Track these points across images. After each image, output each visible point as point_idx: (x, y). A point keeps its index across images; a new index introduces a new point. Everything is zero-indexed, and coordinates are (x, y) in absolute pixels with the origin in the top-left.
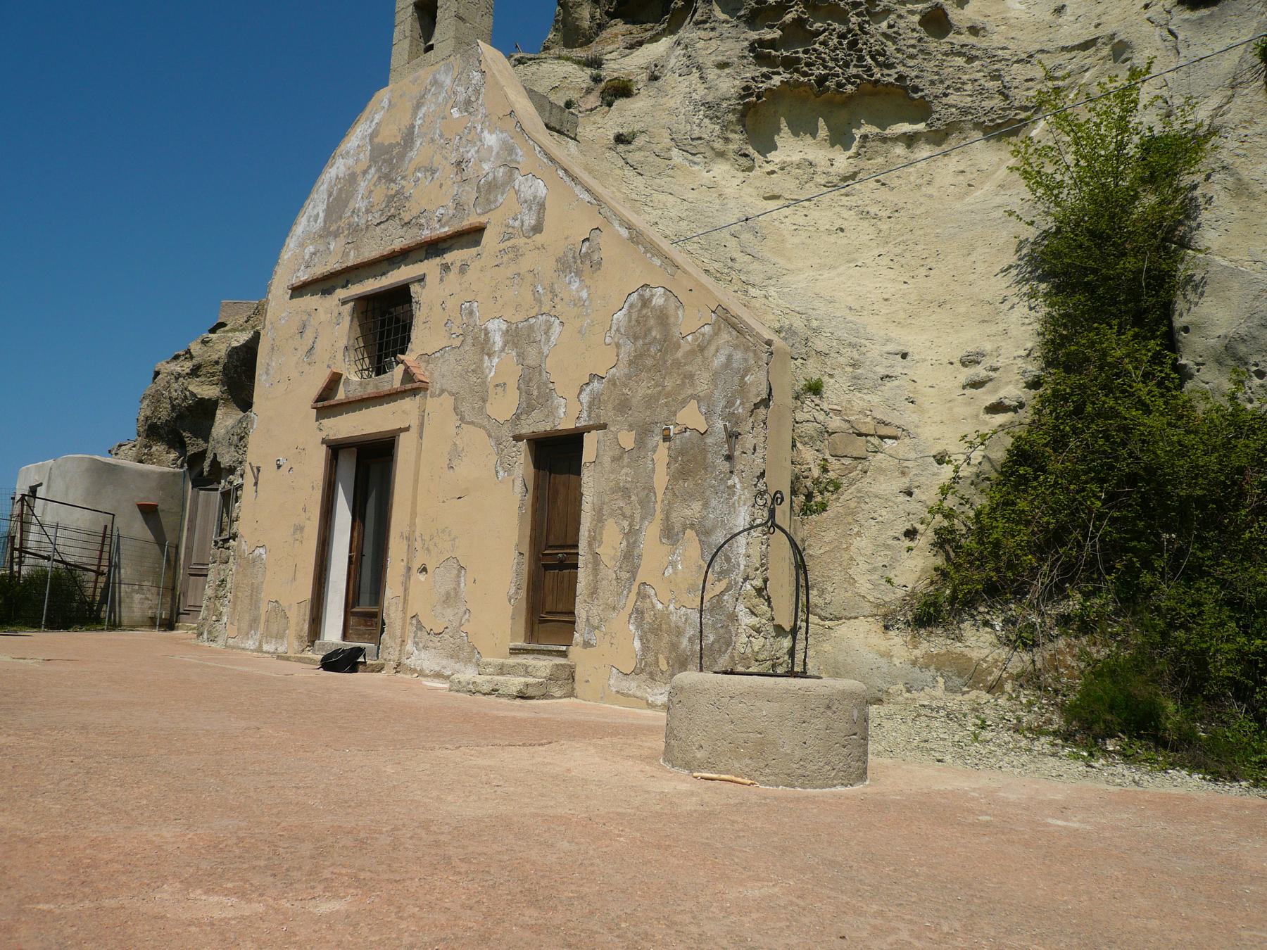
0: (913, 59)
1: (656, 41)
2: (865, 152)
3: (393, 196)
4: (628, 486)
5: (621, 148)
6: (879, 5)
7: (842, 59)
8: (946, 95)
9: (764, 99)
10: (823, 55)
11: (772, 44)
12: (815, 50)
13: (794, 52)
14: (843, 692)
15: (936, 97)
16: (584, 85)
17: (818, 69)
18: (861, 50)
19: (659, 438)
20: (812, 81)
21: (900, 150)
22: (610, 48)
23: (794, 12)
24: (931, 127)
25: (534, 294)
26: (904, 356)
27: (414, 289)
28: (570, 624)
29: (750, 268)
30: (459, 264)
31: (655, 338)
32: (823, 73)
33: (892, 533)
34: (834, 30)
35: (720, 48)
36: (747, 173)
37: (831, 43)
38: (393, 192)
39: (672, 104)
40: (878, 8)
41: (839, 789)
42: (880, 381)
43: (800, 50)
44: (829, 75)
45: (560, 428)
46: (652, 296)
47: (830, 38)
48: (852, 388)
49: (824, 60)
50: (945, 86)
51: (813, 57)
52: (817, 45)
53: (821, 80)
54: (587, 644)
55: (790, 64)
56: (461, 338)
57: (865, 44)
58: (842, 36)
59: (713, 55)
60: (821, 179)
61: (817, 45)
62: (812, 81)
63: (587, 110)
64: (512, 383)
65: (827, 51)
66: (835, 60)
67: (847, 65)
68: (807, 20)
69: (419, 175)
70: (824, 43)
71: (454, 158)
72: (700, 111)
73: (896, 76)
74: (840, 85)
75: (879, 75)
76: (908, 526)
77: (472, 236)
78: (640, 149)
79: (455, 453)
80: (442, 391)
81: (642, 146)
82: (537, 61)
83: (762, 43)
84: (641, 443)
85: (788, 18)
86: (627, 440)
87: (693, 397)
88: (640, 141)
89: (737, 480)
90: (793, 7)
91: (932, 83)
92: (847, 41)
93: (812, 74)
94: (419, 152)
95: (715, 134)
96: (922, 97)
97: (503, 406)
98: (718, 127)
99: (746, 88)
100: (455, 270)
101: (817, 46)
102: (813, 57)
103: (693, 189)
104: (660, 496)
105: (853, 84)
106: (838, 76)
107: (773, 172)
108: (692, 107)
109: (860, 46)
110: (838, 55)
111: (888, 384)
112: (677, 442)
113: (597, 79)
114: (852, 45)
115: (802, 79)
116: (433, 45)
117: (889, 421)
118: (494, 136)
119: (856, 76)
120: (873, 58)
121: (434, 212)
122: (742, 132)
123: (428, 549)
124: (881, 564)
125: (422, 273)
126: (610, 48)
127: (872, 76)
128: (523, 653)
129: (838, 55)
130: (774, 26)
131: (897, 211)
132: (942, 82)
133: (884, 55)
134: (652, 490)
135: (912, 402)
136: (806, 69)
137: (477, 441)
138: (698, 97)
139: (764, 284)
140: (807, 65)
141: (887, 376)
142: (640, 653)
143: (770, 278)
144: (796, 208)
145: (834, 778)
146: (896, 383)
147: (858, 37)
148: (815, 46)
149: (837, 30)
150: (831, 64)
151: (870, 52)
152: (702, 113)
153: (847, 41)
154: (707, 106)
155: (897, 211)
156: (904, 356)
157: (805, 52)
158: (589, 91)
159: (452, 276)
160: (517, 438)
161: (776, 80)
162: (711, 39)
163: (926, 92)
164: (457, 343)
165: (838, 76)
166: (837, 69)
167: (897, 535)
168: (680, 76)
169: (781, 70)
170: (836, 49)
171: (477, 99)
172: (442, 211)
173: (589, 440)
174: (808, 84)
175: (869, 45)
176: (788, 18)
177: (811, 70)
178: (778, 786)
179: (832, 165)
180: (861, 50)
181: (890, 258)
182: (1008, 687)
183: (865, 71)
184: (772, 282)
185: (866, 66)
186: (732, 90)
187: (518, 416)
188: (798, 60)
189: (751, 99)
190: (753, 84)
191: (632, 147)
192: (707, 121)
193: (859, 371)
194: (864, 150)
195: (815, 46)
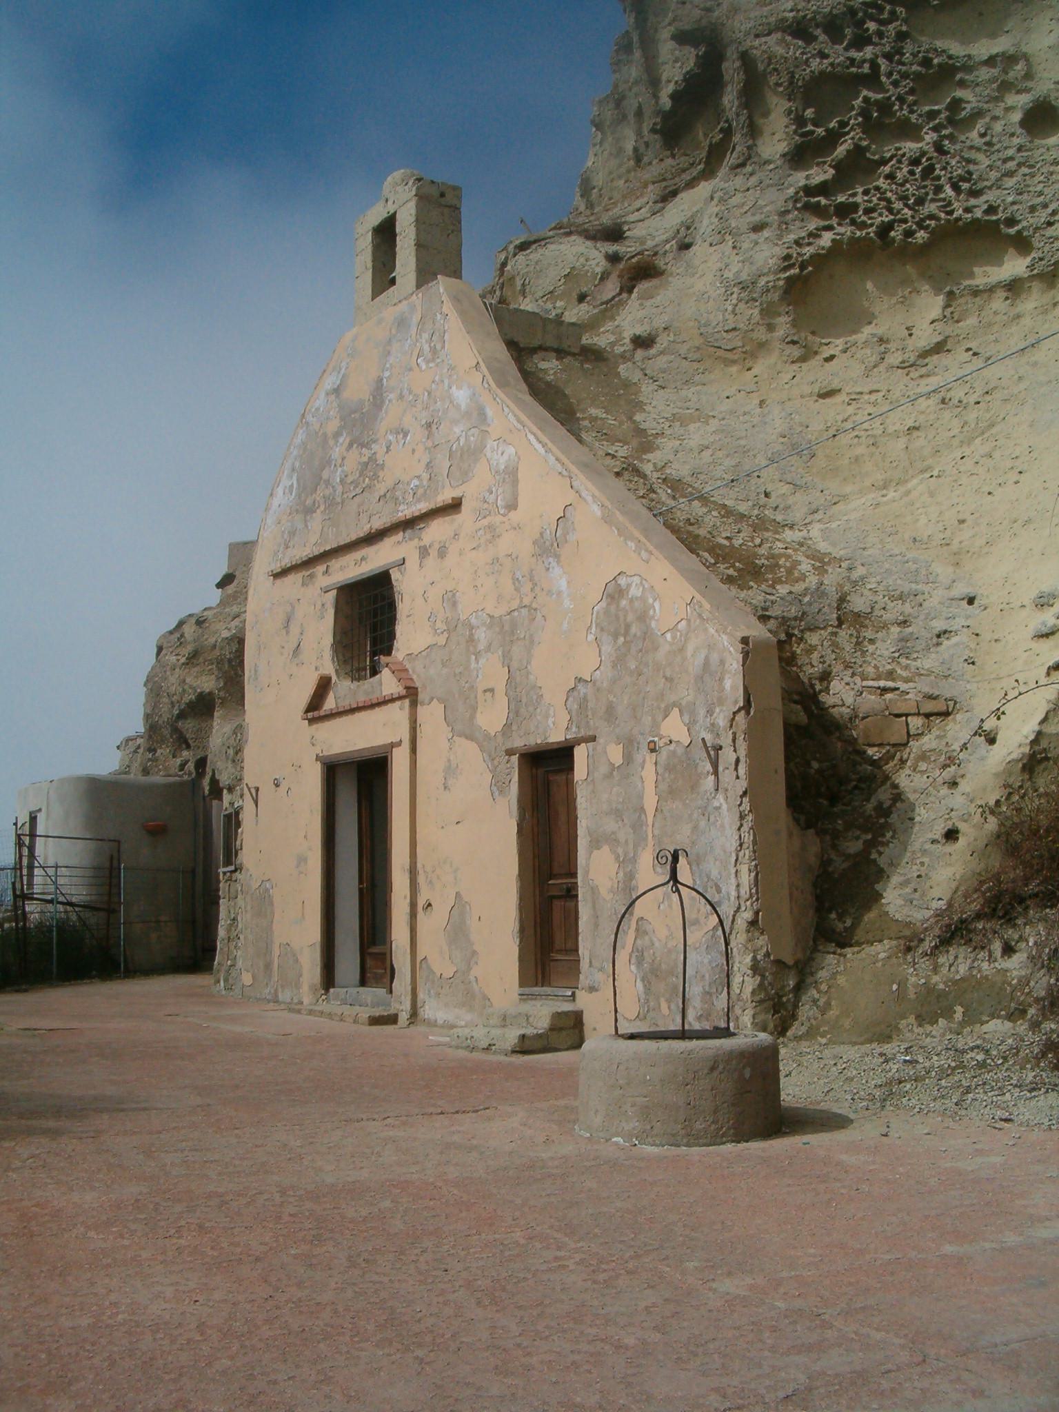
0: (1012, 176)
1: (693, 187)
2: (952, 313)
3: (366, 464)
4: (620, 807)
5: (640, 354)
6: (965, 108)
7: (914, 195)
8: (1050, 224)
9: (810, 268)
10: (889, 194)
11: (824, 189)
12: (877, 188)
13: (850, 195)
14: (731, 1052)
15: (1037, 229)
16: (599, 270)
17: (881, 215)
18: (939, 178)
19: (644, 750)
20: (872, 235)
21: (998, 303)
22: (638, 204)
23: (849, 141)
24: (1032, 270)
25: (514, 584)
26: (971, 601)
27: (395, 575)
28: (574, 967)
29: (791, 501)
30: (437, 546)
31: (635, 635)
32: (887, 220)
33: (931, 836)
34: (904, 155)
35: (761, 202)
36: (799, 365)
37: (899, 175)
38: (365, 459)
39: (699, 286)
40: (964, 113)
41: (729, 1146)
42: (935, 640)
43: (860, 190)
44: (894, 221)
45: (551, 740)
46: (629, 586)
47: (898, 168)
48: (897, 655)
49: (889, 201)
50: (1049, 210)
51: (874, 199)
52: (882, 180)
53: (885, 230)
54: (592, 989)
55: (845, 211)
56: (446, 635)
57: (944, 168)
58: (915, 162)
59: (749, 213)
60: (894, 359)
61: (882, 180)
62: (872, 235)
63: (602, 304)
64: (501, 687)
65: (894, 187)
66: (904, 198)
67: (920, 201)
68: (867, 148)
69: (391, 437)
70: (891, 177)
71: (424, 417)
72: (732, 294)
73: (985, 207)
74: (909, 233)
75: (961, 211)
76: (949, 825)
77: (455, 506)
78: (662, 353)
79: (450, 771)
80: (432, 699)
81: (665, 349)
82: (543, 243)
83: (809, 191)
84: (628, 758)
85: (841, 150)
86: (615, 754)
87: (674, 705)
88: (663, 341)
89: (722, 800)
90: (848, 133)
91: (1033, 209)
92: (920, 168)
93: (872, 225)
94: (392, 414)
95: (752, 322)
96: (1019, 232)
97: (492, 717)
98: (756, 311)
99: (787, 257)
100: (433, 553)
101: (881, 183)
102: (874, 199)
103: (728, 397)
104: (650, 820)
105: (926, 228)
106: (905, 221)
107: (832, 358)
108: (724, 290)
109: (937, 172)
110: (908, 190)
111: (946, 642)
112: (664, 753)
113: (614, 259)
114: (928, 171)
115: (858, 233)
116: (394, 277)
117: (937, 693)
118: (461, 392)
119: (931, 217)
120: (955, 187)
121: (408, 484)
122: (787, 313)
123: (431, 882)
124: (915, 875)
125: (401, 557)
126: (638, 204)
127: (951, 213)
128: (532, 999)
129: (908, 190)
130: (825, 163)
131: (987, 393)
132: (1045, 206)
133: (968, 181)
134: (642, 809)
135: (973, 663)
136: (864, 218)
137: (469, 754)
138: (731, 275)
139: (807, 521)
140: (868, 211)
141: (945, 632)
142: (643, 996)
143: (816, 511)
144: (859, 406)
145: (723, 1136)
146: (954, 640)
147: (934, 161)
148: (877, 183)
149: (908, 155)
150: (898, 205)
151: (951, 178)
152: (735, 296)
153: (920, 168)
154: (741, 286)
155: (987, 393)
156: (971, 601)
157: (866, 193)
158: (604, 276)
159: (431, 561)
160: (510, 753)
161: (826, 239)
162: (748, 190)
163: (1024, 224)
164: (442, 640)
165: (905, 221)
166: (906, 210)
167: (936, 837)
168: (711, 245)
169: (834, 221)
170: (906, 181)
171: (443, 347)
172: (416, 482)
173: (580, 753)
174: (866, 238)
175: (949, 169)
176: (841, 150)
177: (870, 218)
178: (663, 1146)
179: (911, 335)
180: (939, 178)
181: (975, 460)
182: (1032, 1011)
183: (942, 206)
184: (817, 516)
185: (944, 200)
186: (770, 261)
187: (508, 726)
188: (855, 207)
189: (792, 271)
190: (794, 252)
191: (653, 351)
192: (742, 306)
193: (910, 630)
194: (950, 310)
195: (877, 183)
